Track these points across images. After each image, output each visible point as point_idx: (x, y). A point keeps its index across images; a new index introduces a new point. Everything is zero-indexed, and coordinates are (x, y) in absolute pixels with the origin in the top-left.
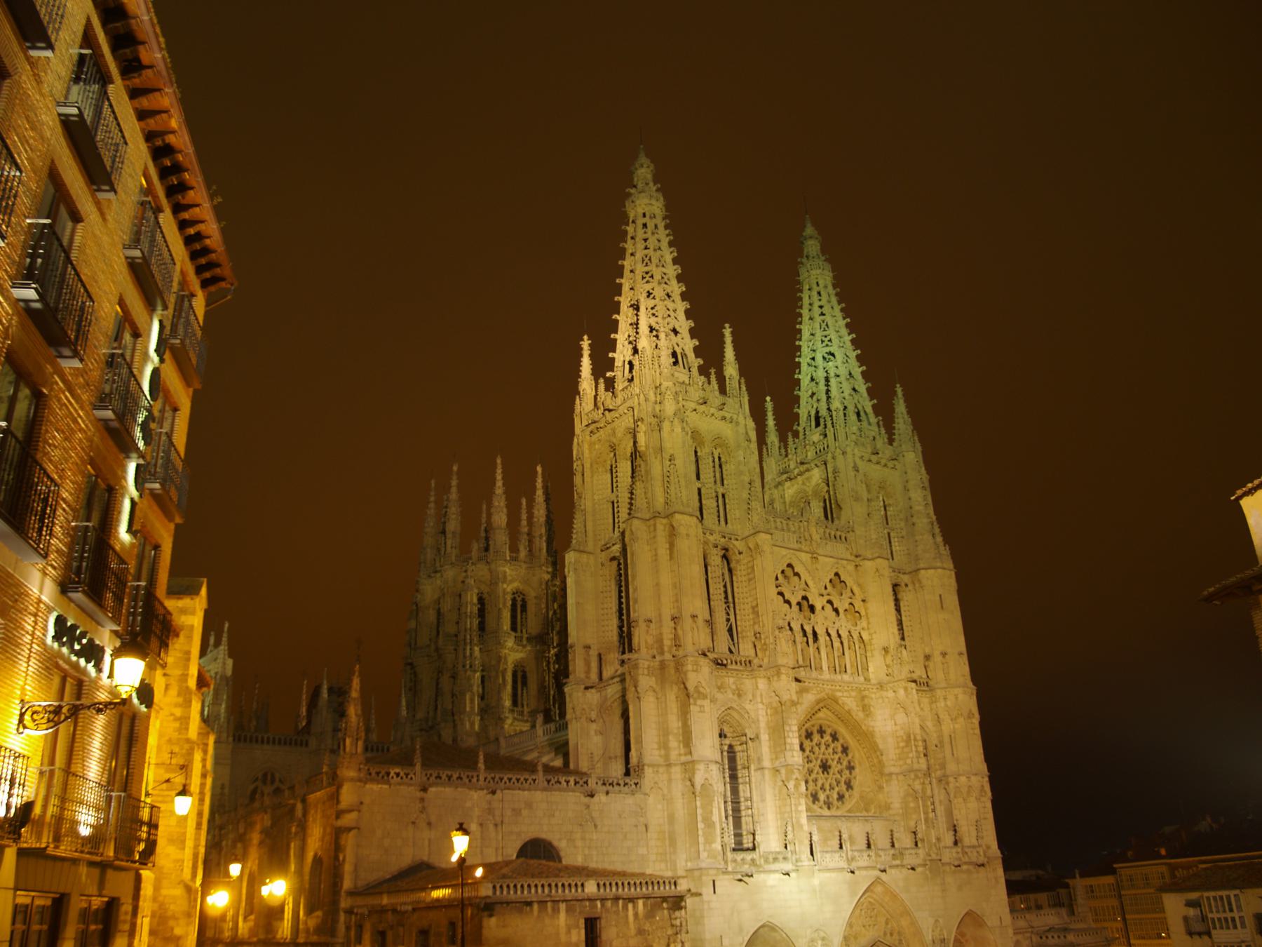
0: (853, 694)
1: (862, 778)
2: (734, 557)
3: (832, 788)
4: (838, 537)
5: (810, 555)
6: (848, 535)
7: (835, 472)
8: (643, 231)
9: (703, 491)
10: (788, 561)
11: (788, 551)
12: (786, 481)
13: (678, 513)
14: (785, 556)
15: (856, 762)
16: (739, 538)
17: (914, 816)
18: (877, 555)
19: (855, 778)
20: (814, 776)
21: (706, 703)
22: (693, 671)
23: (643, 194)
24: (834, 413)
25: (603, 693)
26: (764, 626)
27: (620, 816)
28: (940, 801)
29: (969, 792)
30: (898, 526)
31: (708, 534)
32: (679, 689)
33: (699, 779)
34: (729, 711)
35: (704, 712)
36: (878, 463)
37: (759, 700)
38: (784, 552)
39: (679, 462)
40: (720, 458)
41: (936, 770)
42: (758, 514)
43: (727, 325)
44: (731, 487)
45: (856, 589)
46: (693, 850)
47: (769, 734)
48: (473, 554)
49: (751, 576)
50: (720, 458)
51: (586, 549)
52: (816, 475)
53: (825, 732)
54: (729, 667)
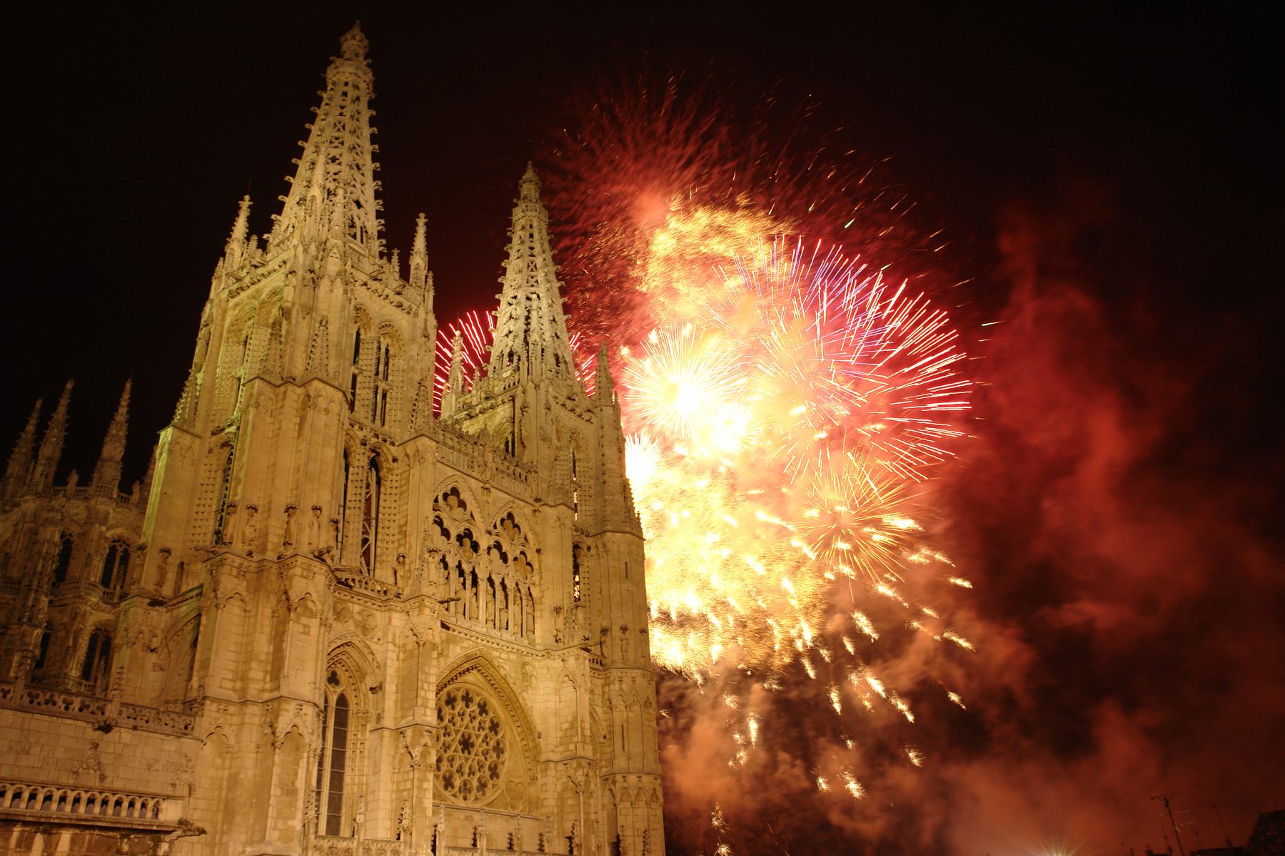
0: (513, 657)
1: (512, 764)
2: (386, 465)
3: (472, 773)
4: (517, 475)
5: (482, 485)
6: (530, 476)
7: (524, 408)
8: (341, 98)
9: (359, 379)
10: (454, 485)
11: (456, 473)
12: (466, 419)
13: (320, 380)
14: (447, 477)
15: (507, 744)
16: (397, 444)
17: (572, 817)
18: (561, 501)
19: (503, 763)
20: (450, 752)
21: (314, 623)
22: (302, 576)
23: (349, 62)
24: (531, 346)
25: (175, 613)
26: (410, 548)
27: (149, 767)
28: (603, 806)
29: (638, 795)
30: (587, 484)
31: (356, 427)
32: (279, 601)
33: (283, 725)
34: (347, 648)
35: (308, 634)
36: (572, 410)
37: (390, 639)
38: (450, 472)
39: (333, 328)
40: (387, 351)
41: (602, 767)
42: (424, 417)
43: (422, 215)
44: (396, 384)
45: (530, 537)
46: (257, 828)
47: (397, 685)
48: (69, 487)
49: (404, 488)
50: (387, 351)
51: (192, 430)
52: (503, 412)
53: (471, 700)
54: (355, 589)
